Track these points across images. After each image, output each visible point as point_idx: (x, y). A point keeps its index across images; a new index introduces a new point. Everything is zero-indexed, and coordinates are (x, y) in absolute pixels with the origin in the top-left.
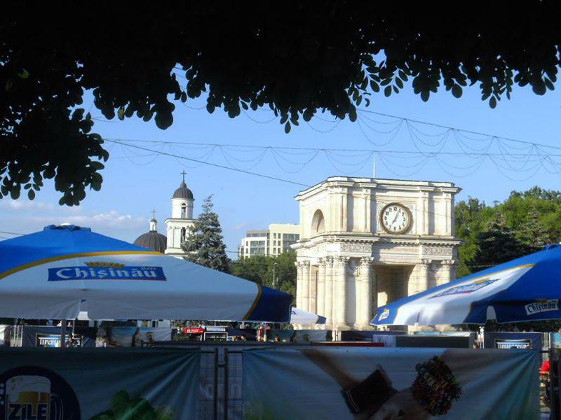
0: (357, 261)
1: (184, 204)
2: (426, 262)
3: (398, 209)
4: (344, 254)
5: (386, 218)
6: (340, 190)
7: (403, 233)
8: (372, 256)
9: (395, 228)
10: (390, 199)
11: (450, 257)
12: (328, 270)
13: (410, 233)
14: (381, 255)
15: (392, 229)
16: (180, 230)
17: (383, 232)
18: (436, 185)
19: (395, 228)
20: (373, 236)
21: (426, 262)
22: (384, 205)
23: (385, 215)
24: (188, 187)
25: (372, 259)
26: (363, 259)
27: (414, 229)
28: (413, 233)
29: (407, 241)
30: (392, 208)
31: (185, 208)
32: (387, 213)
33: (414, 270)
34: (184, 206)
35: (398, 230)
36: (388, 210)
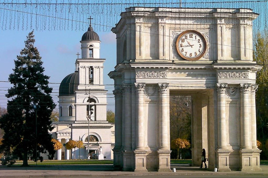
1: (91, 46)
9: (191, 54)
19: (191, 54)
29: (159, 66)
34: (91, 48)
35: (193, 56)
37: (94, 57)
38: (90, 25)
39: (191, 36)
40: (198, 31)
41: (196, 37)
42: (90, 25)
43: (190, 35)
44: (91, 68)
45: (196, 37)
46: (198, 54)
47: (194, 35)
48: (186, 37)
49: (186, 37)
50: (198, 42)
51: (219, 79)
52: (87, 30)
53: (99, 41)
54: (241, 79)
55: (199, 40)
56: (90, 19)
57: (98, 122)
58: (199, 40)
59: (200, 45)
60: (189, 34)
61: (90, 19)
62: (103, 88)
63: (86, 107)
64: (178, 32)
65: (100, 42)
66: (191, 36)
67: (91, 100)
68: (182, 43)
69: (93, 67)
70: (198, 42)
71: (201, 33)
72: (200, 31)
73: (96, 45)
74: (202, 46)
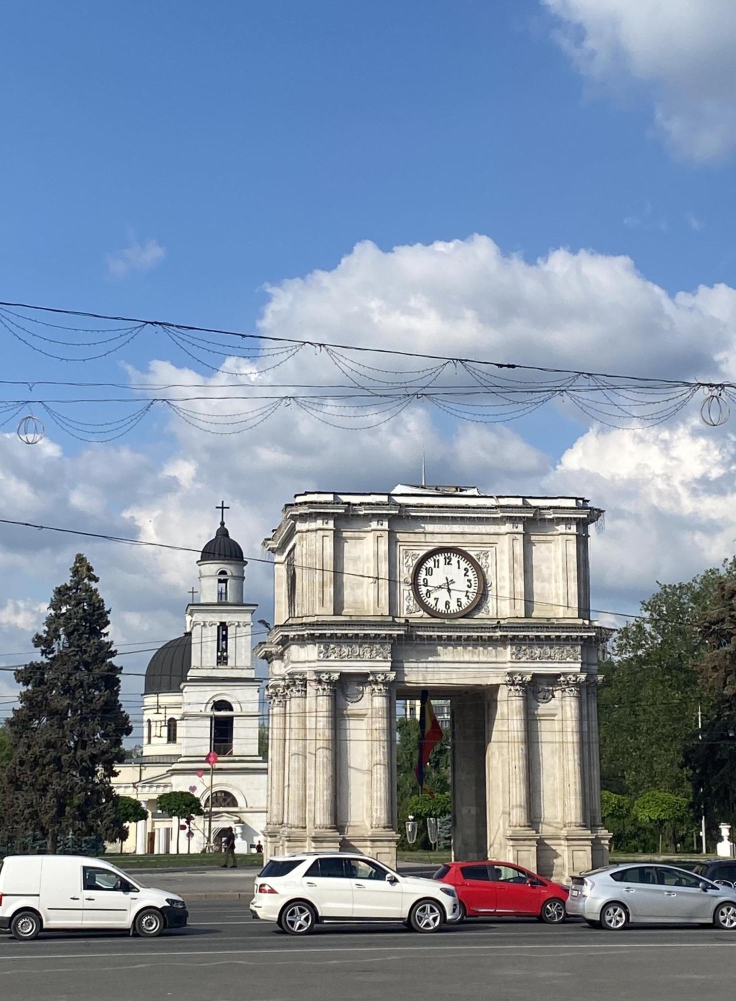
0: (362, 679)
1: (223, 573)
2: (325, 677)
3: (454, 560)
4: (518, 667)
6: (508, 527)
8: (582, 670)
9: (447, 603)
10: (438, 538)
11: (577, 667)
12: (294, 705)
13: (481, 615)
14: (405, 669)
15: (441, 607)
16: (215, 628)
17: (421, 613)
18: (345, 499)
19: (447, 603)
20: (393, 624)
21: (325, 677)
23: (423, 574)
24: (231, 536)
25: (392, 676)
26: (562, 679)
27: (491, 603)
28: (492, 614)
30: (441, 558)
31: (225, 581)
32: (429, 572)
33: (499, 697)
34: (222, 577)
35: (454, 607)
36: (430, 563)
38: (222, 524)
39: (448, 561)
40: (464, 549)
41: (458, 562)
42: (222, 524)
43: (445, 558)
45: (458, 562)
46: (463, 604)
47: (454, 560)
48: (437, 563)
49: (437, 563)
55: (465, 569)
57: (237, 759)
58: (465, 569)
59: (469, 581)
60: (444, 557)
62: (251, 674)
64: (417, 552)
66: (448, 561)
67: (221, 705)
68: (428, 577)
74: (473, 585)
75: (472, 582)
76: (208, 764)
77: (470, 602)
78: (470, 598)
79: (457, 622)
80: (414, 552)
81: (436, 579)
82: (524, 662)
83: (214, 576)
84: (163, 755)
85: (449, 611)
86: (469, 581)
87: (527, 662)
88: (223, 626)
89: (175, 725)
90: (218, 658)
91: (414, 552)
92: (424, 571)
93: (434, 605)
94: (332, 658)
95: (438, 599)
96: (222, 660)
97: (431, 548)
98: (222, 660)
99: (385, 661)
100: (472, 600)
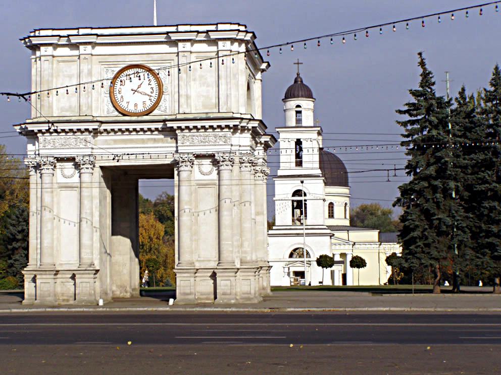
1: (298, 106)
5: (119, 92)
7: (148, 113)
9: (136, 105)
10: (128, 58)
19: (136, 105)
22: (117, 70)
28: (168, 112)
34: (299, 109)
37: (304, 124)
38: (298, 75)
40: (148, 65)
42: (298, 75)
44: (298, 142)
50: (149, 84)
51: (180, 146)
52: (293, 82)
53: (313, 98)
54: (218, 145)
56: (298, 63)
59: (152, 88)
61: (298, 63)
63: (290, 203)
65: (313, 100)
69: (301, 140)
70: (149, 84)
71: (153, 68)
72: (151, 65)
73: (307, 105)
74: (155, 91)
75: (154, 89)
76: (329, 230)
77: (153, 104)
78: (152, 101)
79: (140, 118)
80: (112, 69)
81: (146, 88)
82: (187, 146)
83: (293, 109)
84: (344, 226)
85: (137, 111)
86: (152, 88)
87: (190, 146)
88: (298, 142)
89: (333, 207)
90: (296, 162)
91: (112, 69)
92: (119, 82)
93: (126, 107)
94: (49, 147)
95: (129, 102)
96: (299, 163)
97: (124, 66)
98: (299, 163)
99: (86, 148)
100: (154, 102)
